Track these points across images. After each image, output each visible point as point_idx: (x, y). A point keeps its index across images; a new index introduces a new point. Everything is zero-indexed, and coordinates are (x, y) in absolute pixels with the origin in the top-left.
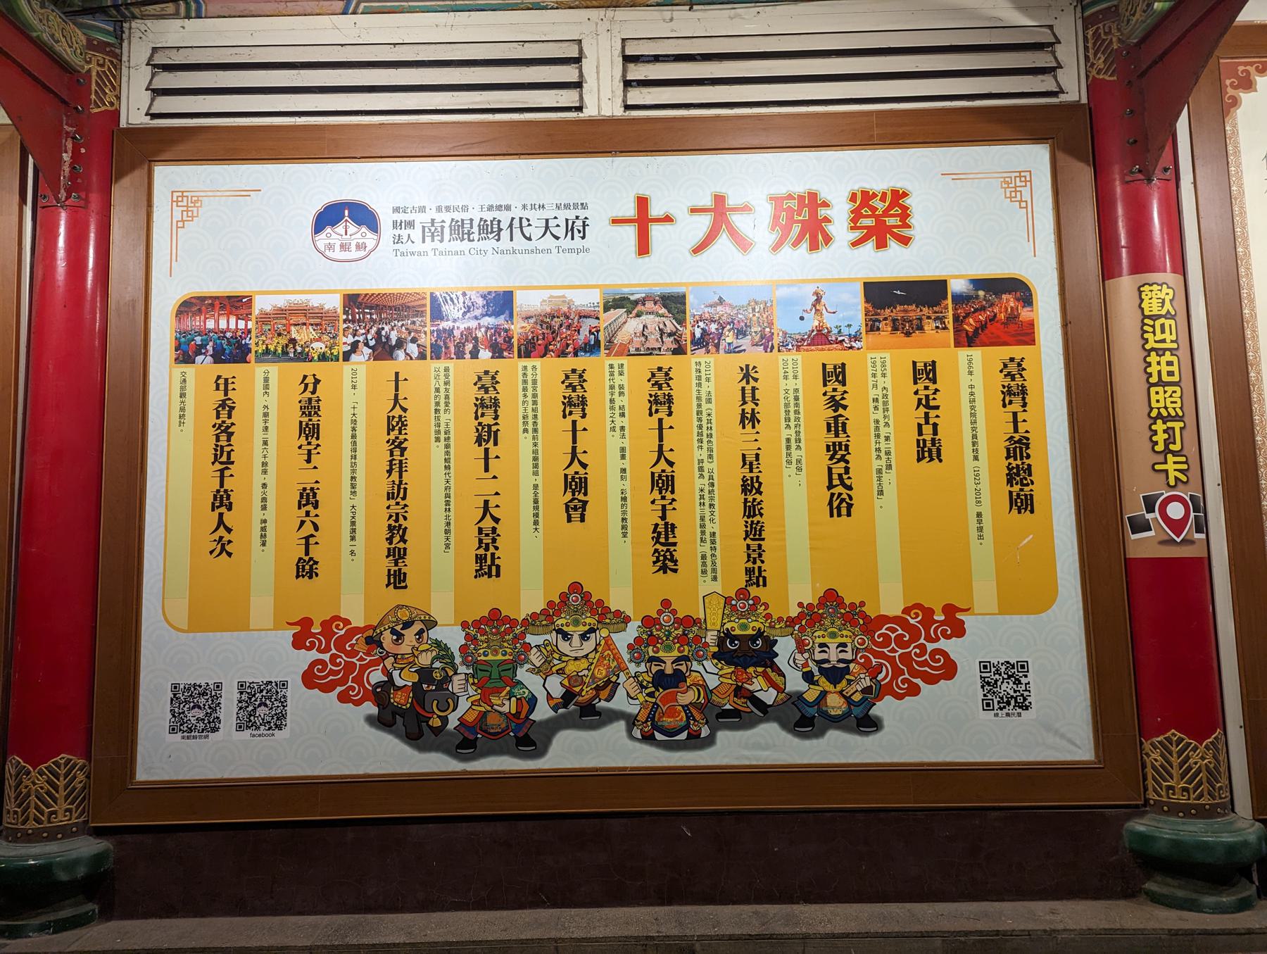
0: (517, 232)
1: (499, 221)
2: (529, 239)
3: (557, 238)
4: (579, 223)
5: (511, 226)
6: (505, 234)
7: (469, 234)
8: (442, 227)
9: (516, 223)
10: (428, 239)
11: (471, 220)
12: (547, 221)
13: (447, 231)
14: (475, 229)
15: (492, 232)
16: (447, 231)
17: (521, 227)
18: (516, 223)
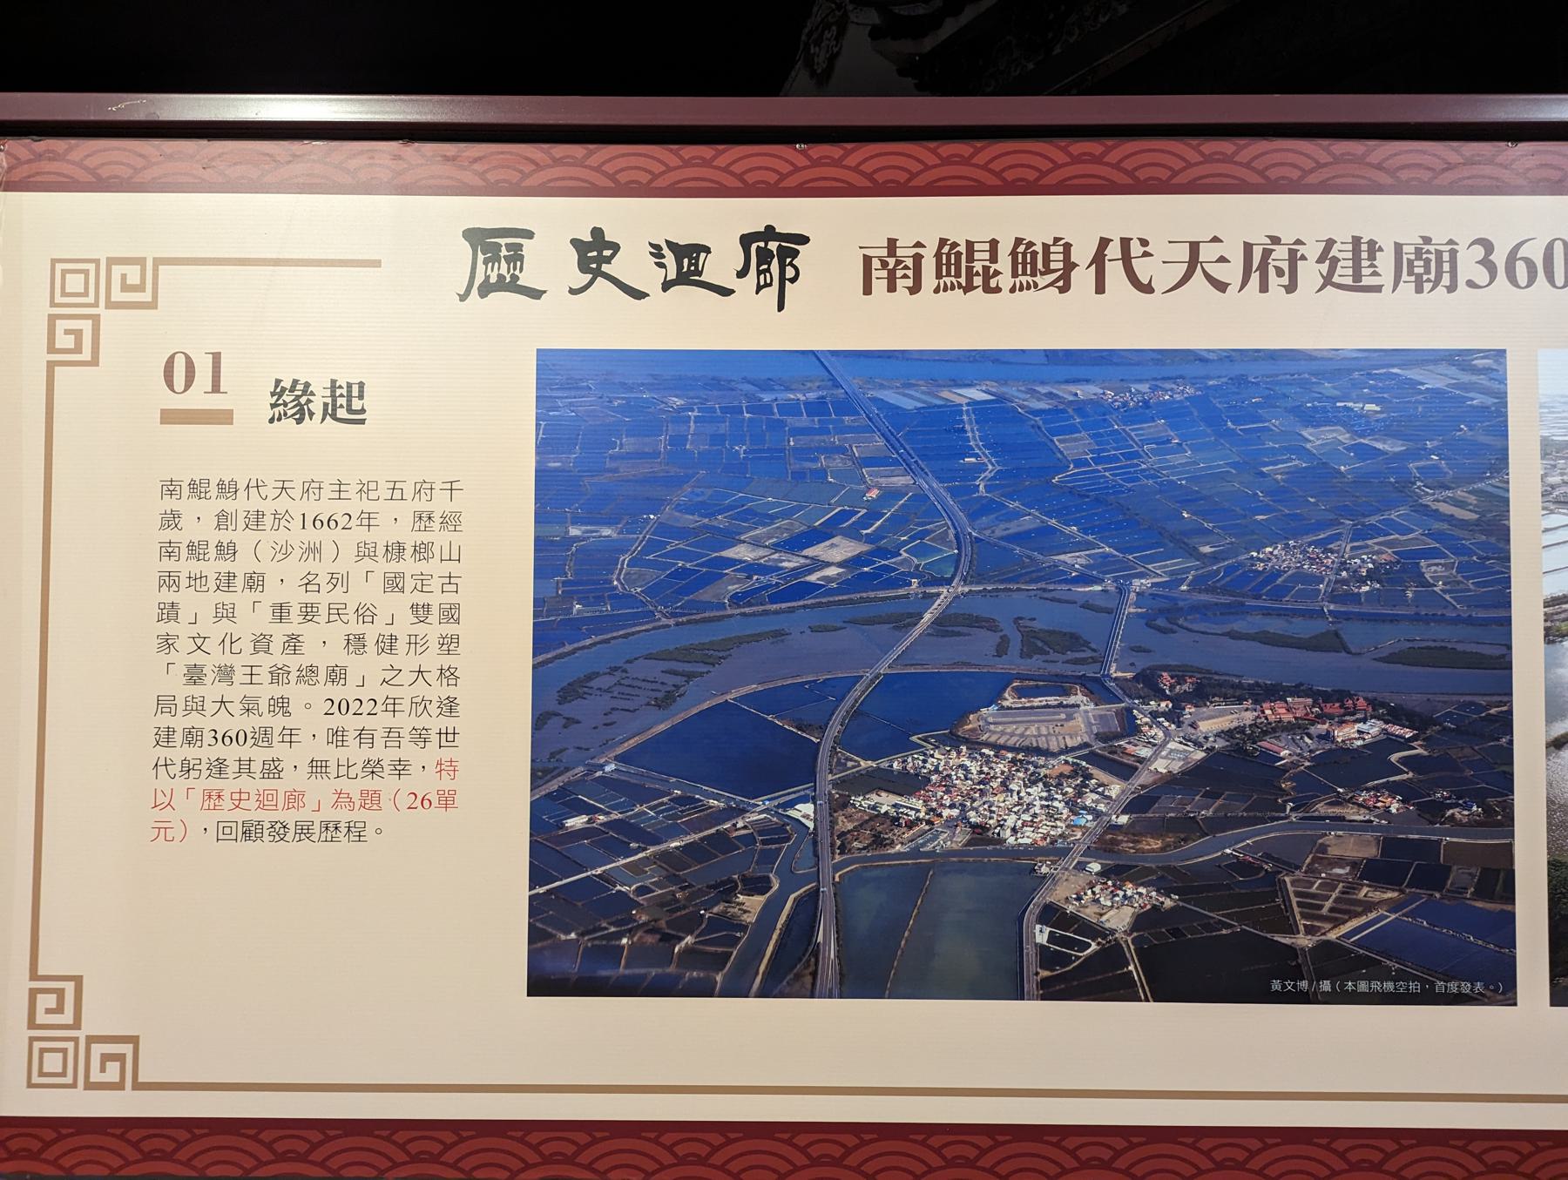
0: (1115, 271)
1: (1067, 246)
2: (1147, 289)
3: (1221, 286)
4: (1281, 253)
5: (1099, 260)
6: (1083, 277)
7: (987, 275)
8: (918, 259)
9: (1114, 251)
10: (880, 285)
11: (994, 244)
12: (1194, 247)
13: (928, 266)
14: (1004, 263)
15: (1048, 271)
16: (928, 266)
17: (1126, 258)
18: (1114, 251)
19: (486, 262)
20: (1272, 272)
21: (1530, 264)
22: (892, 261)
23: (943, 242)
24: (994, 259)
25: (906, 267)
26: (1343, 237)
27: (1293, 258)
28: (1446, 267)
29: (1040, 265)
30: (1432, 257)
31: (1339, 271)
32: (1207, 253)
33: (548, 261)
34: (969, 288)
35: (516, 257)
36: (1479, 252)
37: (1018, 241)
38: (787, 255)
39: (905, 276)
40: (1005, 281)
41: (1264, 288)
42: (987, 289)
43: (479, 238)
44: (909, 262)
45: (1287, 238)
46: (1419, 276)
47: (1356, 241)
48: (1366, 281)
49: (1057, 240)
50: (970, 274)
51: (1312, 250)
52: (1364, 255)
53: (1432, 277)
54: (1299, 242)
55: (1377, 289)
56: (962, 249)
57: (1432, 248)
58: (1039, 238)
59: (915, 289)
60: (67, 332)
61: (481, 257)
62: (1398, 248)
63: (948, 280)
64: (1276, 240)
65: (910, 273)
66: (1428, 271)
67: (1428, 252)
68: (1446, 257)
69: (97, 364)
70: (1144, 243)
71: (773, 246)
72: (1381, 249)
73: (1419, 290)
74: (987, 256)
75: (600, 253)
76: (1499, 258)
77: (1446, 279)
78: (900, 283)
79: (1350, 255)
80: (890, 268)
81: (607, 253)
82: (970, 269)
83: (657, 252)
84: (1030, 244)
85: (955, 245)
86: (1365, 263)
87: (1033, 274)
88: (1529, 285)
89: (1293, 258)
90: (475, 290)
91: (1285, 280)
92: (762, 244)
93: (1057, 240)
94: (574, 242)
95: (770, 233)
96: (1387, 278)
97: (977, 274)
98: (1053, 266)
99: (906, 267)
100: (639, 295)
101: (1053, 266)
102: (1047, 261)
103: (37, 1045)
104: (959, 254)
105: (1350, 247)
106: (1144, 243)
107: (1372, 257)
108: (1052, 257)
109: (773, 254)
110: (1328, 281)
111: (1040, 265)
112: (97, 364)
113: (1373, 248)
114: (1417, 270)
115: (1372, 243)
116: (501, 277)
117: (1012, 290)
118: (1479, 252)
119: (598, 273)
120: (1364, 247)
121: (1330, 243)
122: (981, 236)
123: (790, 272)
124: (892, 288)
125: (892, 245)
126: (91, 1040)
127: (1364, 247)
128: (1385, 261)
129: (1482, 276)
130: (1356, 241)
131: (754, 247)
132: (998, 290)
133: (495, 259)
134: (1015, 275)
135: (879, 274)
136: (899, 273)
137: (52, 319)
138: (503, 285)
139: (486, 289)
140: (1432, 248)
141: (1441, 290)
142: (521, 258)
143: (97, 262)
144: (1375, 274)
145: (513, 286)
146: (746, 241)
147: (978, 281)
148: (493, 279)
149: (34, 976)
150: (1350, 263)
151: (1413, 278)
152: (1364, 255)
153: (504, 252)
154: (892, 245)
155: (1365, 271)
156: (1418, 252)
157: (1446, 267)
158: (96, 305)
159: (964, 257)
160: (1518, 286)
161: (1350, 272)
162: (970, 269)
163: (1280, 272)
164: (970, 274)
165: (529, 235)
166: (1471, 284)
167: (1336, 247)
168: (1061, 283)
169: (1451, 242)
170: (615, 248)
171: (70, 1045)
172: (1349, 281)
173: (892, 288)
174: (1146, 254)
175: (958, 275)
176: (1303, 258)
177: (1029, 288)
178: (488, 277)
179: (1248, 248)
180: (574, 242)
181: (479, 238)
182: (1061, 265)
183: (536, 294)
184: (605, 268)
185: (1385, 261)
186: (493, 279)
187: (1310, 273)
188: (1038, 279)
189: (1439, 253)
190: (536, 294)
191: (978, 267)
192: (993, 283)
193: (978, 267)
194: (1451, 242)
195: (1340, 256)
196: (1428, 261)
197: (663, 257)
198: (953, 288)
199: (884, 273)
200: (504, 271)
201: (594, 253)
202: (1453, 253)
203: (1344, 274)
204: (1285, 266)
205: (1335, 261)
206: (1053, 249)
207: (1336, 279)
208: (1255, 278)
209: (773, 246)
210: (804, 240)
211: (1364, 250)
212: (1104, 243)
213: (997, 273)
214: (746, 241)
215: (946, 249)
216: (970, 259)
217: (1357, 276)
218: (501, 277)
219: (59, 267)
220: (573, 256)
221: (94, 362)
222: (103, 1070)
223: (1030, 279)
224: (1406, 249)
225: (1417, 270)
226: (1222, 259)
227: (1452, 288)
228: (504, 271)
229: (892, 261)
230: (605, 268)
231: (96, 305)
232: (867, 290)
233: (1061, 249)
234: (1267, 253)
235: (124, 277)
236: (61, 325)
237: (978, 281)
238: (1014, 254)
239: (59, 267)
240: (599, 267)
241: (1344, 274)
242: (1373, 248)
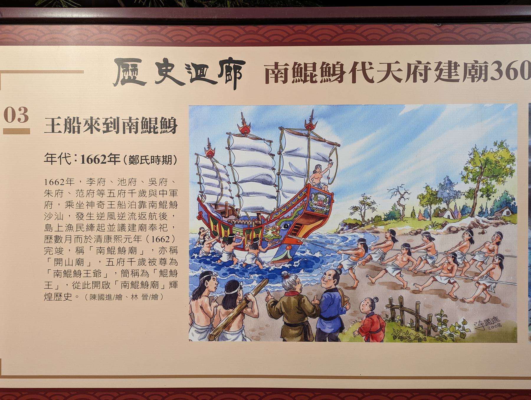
0: (359, 74)
1: (342, 65)
2: (372, 81)
3: (399, 80)
4: (421, 67)
5: (354, 71)
6: (347, 77)
7: (312, 76)
8: (286, 70)
9: (359, 67)
10: (272, 80)
11: (314, 64)
12: (389, 65)
14: (318, 72)
15: (334, 74)
17: (364, 70)
18: (359, 67)
19: (123, 71)
20: (418, 74)
21: (515, 70)
22: (276, 71)
23: (295, 64)
24: (314, 70)
25: (282, 73)
26: (445, 61)
27: (426, 69)
28: (483, 72)
29: (332, 73)
30: (478, 68)
31: (443, 74)
32: (394, 67)
33: (148, 71)
34: (305, 81)
35: (135, 69)
36: (496, 66)
37: (324, 63)
38: (237, 69)
39: (281, 77)
40: (319, 78)
41: (415, 80)
42: (312, 81)
43: (121, 62)
44: (283, 71)
45: (424, 62)
46: (473, 76)
47: (450, 62)
48: (453, 78)
49: (338, 63)
50: (306, 76)
51: (433, 66)
52: (453, 68)
53: (478, 76)
54: (428, 63)
55: (457, 81)
56: (303, 66)
57: (478, 65)
58: (331, 62)
59: (285, 81)
61: (121, 69)
62: (466, 65)
63: (297, 78)
64: (419, 62)
65: (283, 75)
66: (476, 74)
67: (477, 66)
68: (483, 68)
70: (370, 64)
71: (232, 65)
72: (459, 66)
73: (473, 81)
74: (312, 69)
75: (167, 68)
76: (504, 68)
77: (483, 77)
78: (279, 79)
79: (447, 68)
80: (275, 73)
81: (169, 68)
82: (305, 74)
83: (188, 67)
84: (328, 64)
85: (300, 65)
86: (453, 71)
87: (329, 76)
88: (514, 79)
89: (426, 69)
90: (119, 82)
91: (423, 78)
92: (228, 64)
93: (338, 63)
94: (157, 64)
95: (230, 60)
96: (461, 76)
97: (308, 76)
98: (336, 73)
99: (282, 73)
100: (182, 84)
101: (336, 73)
102: (334, 71)
104: (301, 68)
105: (447, 65)
106: (370, 64)
107: (456, 68)
108: (336, 69)
109: (232, 69)
110: (439, 78)
111: (332, 73)
113: (456, 65)
114: (472, 73)
115: (456, 63)
117: (321, 82)
118: (496, 66)
119: (166, 76)
120: (453, 65)
121: (440, 63)
122: (310, 61)
123: (238, 75)
124: (276, 81)
125: (276, 64)
127: (453, 65)
128: (461, 70)
129: (496, 75)
130: (450, 62)
131: (225, 65)
132: (316, 82)
134: (322, 76)
135: (271, 76)
136: (279, 76)
139: (124, 82)
140: (478, 65)
141: (481, 81)
144: (457, 75)
145: (134, 80)
146: (222, 63)
147: (308, 78)
148: (126, 78)
150: (447, 71)
151: (471, 76)
152: (453, 68)
153: (130, 68)
154: (276, 64)
155: (453, 74)
156: (473, 67)
157: (483, 72)
159: (303, 69)
160: (510, 79)
161: (447, 74)
162: (305, 74)
163: (421, 75)
164: (306, 76)
165: (140, 61)
166: (493, 78)
167: (442, 65)
168: (339, 79)
169: (485, 62)
172: (447, 78)
173: (276, 81)
174: (371, 68)
175: (301, 76)
176: (430, 69)
177: (327, 81)
178: (124, 77)
179: (409, 65)
180: (157, 64)
181: (121, 62)
182: (339, 72)
183: (143, 84)
184: (169, 73)
185: (461, 70)
187: (432, 75)
188: (331, 78)
189: (481, 67)
190: (143, 84)
191: (308, 73)
192: (314, 79)
193: (308, 73)
194: (485, 62)
195: (444, 68)
196: (476, 70)
197: (191, 69)
198: (299, 81)
199: (274, 76)
200: (130, 75)
201: (165, 68)
202: (486, 67)
203: (445, 75)
204: (423, 72)
205: (442, 70)
206: (336, 66)
207: (442, 77)
208: (412, 76)
209: (232, 65)
210: (243, 63)
211: (452, 66)
212: (356, 64)
213: (316, 75)
214: (222, 63)
215: (296, 66)
216: (306, 70)
217: (450, 76)
220: (157, 69)
223: (328, 78)
224: (468, 65)
225: (472, 73)
226: (399, 70)
227: (485, 80)
228: (130, 75)
229: (276, 71)
230: (169, 73)
232: (267, 82)
233: (339, 66)
234: (416, 67)
237: (308, 78)
238: (322, 68)
240: (166, 73)
241: (445, 75)
242: (456, 65)
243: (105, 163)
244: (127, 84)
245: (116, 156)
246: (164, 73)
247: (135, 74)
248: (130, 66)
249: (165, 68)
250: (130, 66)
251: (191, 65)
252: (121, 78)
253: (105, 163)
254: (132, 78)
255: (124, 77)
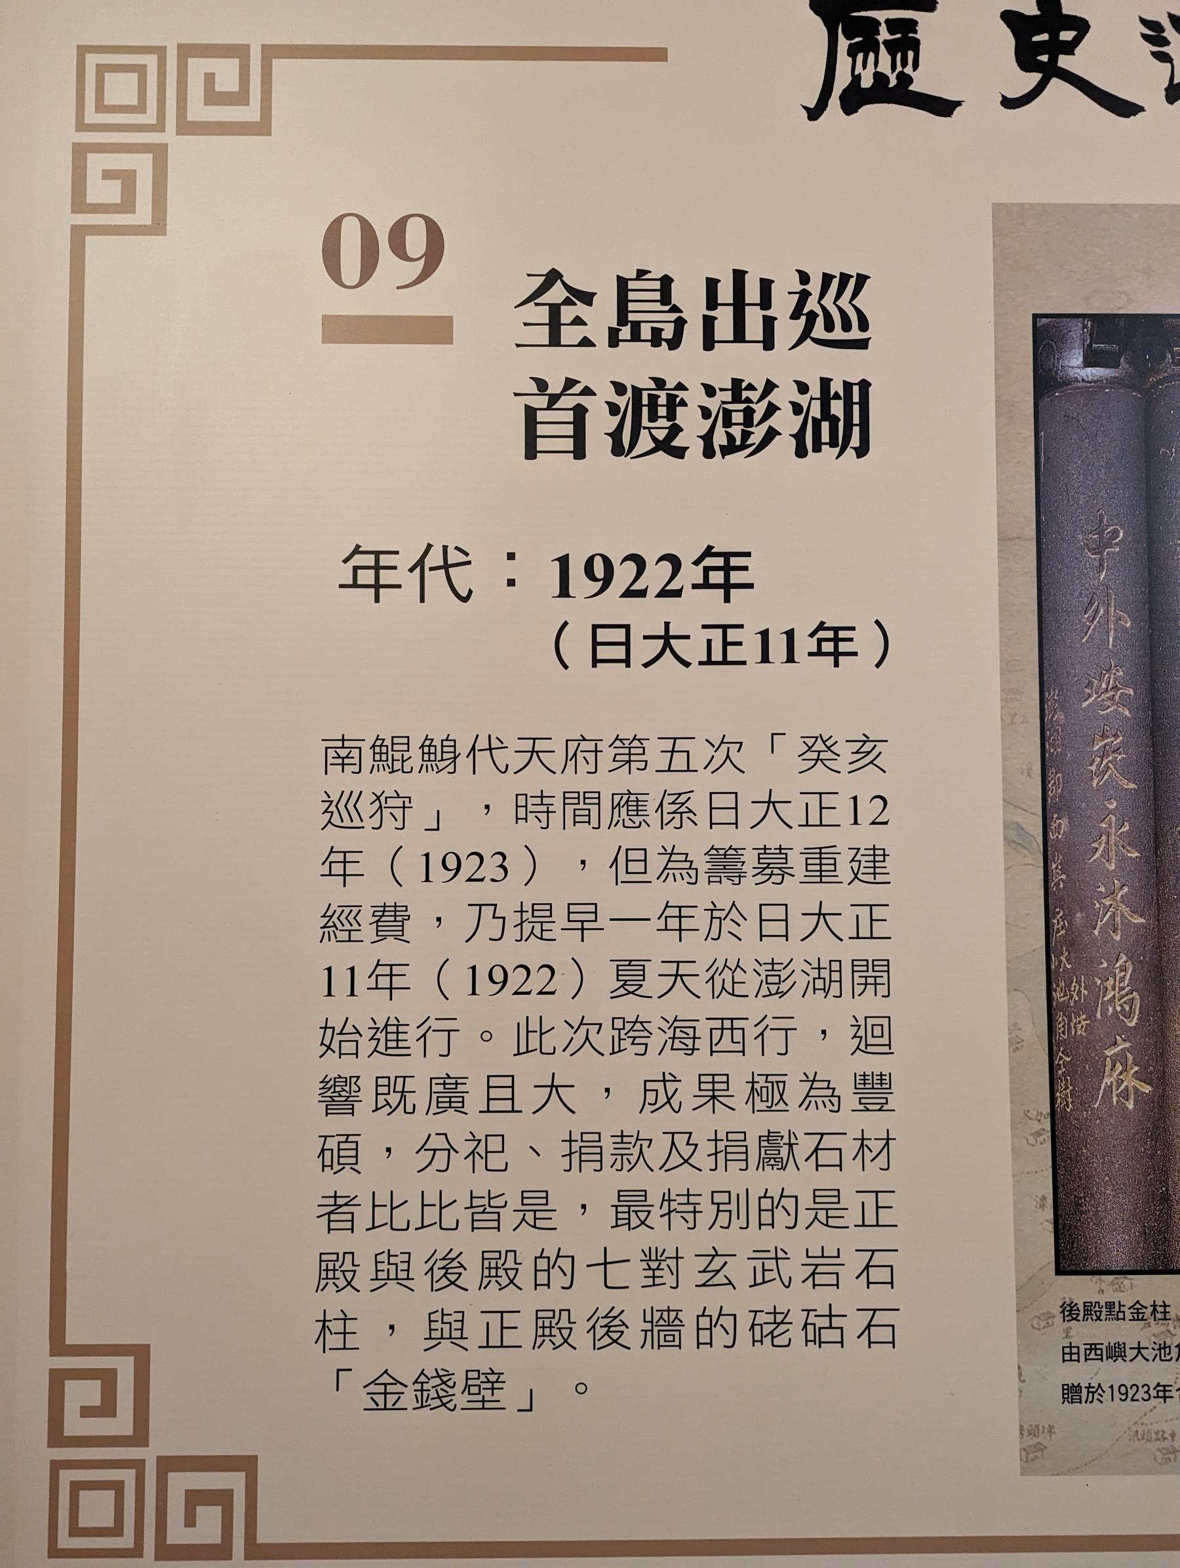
19: (852, 52)
60: (108, 175)
61: (843, 44)
69: (163, 232)
75: (1054, 36)
81: (1067, 36)
90: (834, 102)
94: (1009, 17)
100: (1125, 108)
103: (67, 1477)
112: (163, 232)
116: (880, 78)
119: (1051, 71)
126: (167, 1465)
133: (866, 46)
137: (80, 153)
138: (882, 92)
139: (854, 100)
142: (915, 45)
143: (161, 52)
145: (901, 93)
148: (867, 82)
149: (58, 1346)
153: (884, 35)
158: (160, 127)
170: (1081, 26)
171: (128, 1476)
178: (856, 79)
180: (1009, 17)
183: (943, 107)
184: (1064, 61)
186: (867, 82)
190: (943, 107)
197: (1166, 42)
218: (880, 78)
219: (92, 60)
220: (1007, 40)
221: (158, 227)
222: (190, 1521)
230: (1064, 61)
231: (160, 127)
235: (210, 78)
236: (96, 163)
239: (92, 60)
240: (1054, 60)
243: (678, 593)
244: (866, 110)
245: (734, 561)
246: (1044, 58)
247: (904, 64)
248: (883, 29)
249: (1045, 37)
250: (883, 29)
251: (1166, 23)
252: (842, 81)
253: (678, 593)
254: (893, 82)
255: (856, 79)
